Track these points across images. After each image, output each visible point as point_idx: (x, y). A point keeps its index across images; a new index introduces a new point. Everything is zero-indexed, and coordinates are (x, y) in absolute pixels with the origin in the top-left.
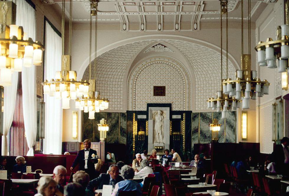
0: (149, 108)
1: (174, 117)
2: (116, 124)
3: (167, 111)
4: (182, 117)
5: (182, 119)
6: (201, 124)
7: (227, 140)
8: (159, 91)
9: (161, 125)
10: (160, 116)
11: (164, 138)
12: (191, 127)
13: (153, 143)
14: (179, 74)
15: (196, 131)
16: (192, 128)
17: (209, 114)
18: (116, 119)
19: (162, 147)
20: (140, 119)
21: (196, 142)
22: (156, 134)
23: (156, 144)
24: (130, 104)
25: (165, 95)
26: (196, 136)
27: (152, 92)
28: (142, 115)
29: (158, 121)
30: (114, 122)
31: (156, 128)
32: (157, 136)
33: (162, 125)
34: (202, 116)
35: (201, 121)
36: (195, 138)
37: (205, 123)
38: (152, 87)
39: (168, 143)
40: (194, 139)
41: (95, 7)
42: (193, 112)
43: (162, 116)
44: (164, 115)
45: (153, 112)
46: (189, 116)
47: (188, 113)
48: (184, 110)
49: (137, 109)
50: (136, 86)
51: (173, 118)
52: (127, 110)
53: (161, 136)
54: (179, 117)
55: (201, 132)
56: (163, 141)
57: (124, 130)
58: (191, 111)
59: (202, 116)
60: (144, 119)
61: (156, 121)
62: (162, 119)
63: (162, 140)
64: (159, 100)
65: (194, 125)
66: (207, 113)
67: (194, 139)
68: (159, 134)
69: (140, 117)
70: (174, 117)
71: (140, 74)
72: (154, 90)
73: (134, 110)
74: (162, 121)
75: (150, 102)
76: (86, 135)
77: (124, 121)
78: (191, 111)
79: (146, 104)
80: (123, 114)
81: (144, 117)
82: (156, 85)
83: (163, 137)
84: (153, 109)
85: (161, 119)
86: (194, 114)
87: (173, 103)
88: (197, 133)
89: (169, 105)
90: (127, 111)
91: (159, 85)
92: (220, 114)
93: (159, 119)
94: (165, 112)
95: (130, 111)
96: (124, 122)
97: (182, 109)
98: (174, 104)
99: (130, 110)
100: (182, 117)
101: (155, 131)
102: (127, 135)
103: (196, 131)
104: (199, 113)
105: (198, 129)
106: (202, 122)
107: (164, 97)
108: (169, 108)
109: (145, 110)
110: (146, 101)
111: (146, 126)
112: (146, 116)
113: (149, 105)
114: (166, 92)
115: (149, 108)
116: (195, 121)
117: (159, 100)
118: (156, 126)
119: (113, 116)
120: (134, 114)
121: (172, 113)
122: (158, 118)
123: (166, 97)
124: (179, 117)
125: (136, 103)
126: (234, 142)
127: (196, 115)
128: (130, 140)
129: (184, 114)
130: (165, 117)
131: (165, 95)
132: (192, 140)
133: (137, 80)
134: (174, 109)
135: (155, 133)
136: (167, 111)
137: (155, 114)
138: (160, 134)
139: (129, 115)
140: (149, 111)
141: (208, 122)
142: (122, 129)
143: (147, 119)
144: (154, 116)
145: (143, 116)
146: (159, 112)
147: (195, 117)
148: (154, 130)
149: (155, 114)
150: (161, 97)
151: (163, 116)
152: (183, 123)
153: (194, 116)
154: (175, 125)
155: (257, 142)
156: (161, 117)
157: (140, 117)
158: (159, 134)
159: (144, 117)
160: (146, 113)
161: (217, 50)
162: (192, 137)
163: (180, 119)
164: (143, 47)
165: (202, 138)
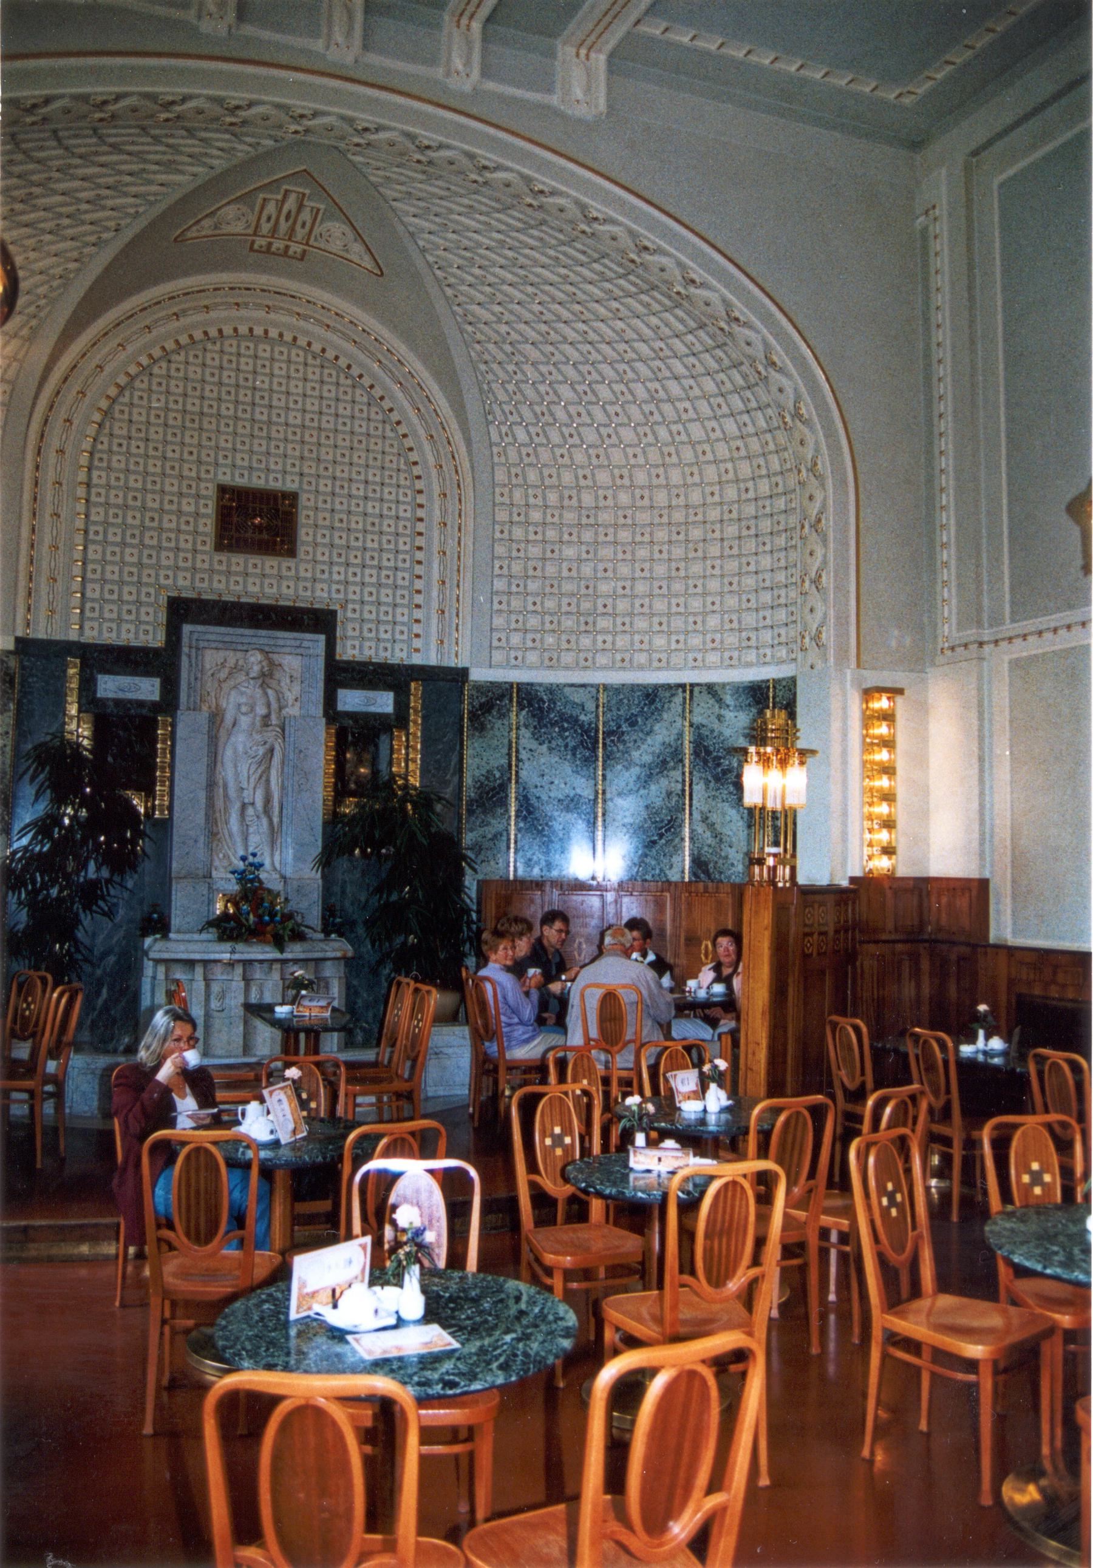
1: (351, 700)
4: (402, 706)
5: (400, 719)
6: (524, 755)
8: (257, 520)
10: (259, 692)
14: (388, 427)
16: (468, 780)
17: (577, 697)
20: (117, 702)
25: (292, 553)
27: (208, 526)
28: (134, 673)
31: (227, 772)
33: (272, 751)
34: (530, 704)
35: (526, 739)
36: (486, 845)
37: (550, 749)
38: (209, 491)
45: (211, 658)
48: (417, 660)
49: (91, 636)
50: (95, 474)
51: (340, 707)
54: (384, 702)
56: (277, 858)
58: (464, 672)
59: (530, 704)
60: (141, 704)
66: (567, 690)
67: (478, 848)
69: (109, 686)
70: (351, 700)
71: (127, 393)
72: (224, 517)
73: (73, 636)
75: (185, 586)
78: (464, 672)
79: (163, 601)
81: (148, 689)
82: (240, 482)
85: (261, 710)
86: (479, 687)
87: (344, 607)
88: (500, 811)
90: (18, 640)
91: (258, 482)
92: (653, 702)
93: (252, 709)
104: (511, 684)
105: (503, 787)
106: (534, 745)
108: (322, 638)
109: (156, 639)
111: (155, 750)
112: (157, 682)
121: (340, 674)
124: (384, 702)
127: (495, 699)
133: (106, 431)
134: (349, 651)
135: (219, 804)
136: (300, 659)
137: (223, 675)
141: (572, 744)
143: (169, 703)
144: (210, 685)
145: (137, 679)
147: (487, 707)
149: (223, 675)
150: (270, 564)
153: (482, 705)
156: (266, 694)
157: (109, 686)
160: (160, 662)
163: (387, 715)
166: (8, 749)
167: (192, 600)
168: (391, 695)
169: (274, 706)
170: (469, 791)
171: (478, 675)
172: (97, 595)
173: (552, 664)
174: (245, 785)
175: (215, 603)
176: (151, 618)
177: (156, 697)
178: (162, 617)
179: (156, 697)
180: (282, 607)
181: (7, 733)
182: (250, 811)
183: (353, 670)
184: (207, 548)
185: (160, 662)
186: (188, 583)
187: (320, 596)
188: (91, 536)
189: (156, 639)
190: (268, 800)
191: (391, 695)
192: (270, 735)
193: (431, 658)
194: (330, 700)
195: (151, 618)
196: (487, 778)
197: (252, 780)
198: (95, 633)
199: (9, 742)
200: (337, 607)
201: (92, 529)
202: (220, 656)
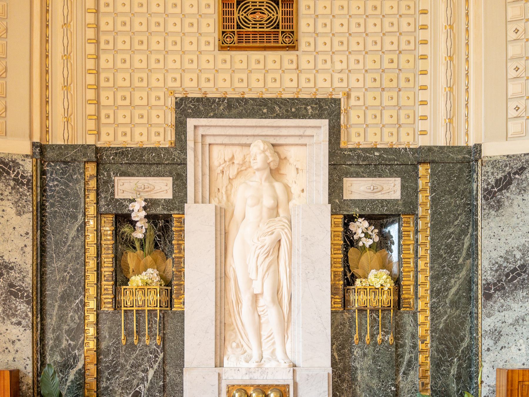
0: (191, 122)
3: (308, 147)
9: (268, 240)
10: (266, 185)
11: (296, 329)
12: (473, 252)
13: (219, 364)
22: (238, 301)
24: (57, 109)
25: (293, 47)
26: (510, 316)
29: (252, 214)
31: (236, 263)
32: (244, 316)
36: (506, 330)
40: (497, 335)
43: (278, 186)
44: (289, 173)
45: (219, 155)
47: (456, 166)
48: (423, 142)
49: (108, 139)
52: (36, 139)
53: (271, 316)
54: (390, 189)
56: (288, 346)
57: (12, 273)
61: (238, 214)
62: (276, 199)
63: (277, 339)
67: (497, 335)
68: (255, 298)
73: (91, 140)
74: (278, 215)
77: (11, 211)
79: (171, 102)
81: (162, 188)
84: (215, 142)
85: (268, 202)
87: (348, 96)
89: (328, 109)
93: (259, 201)
94: (293, 153)
95: (53, 147)
96: (16, 220)
97: (407, 139)
98: (353, 102)
99: (57, 138)
100: (410, 191)
101: (232, 283)
102: (41, 312)
107: (288, 56)
109: (164, 139)
110: (170, 84)
112: (169, 180)
115: (191, 122)
116: (507, 211)
120: (91, 169)
121: (343, 163)
122: (249, 197)
123: (304, 56)
124: (390, 189)
125: (103, 94)
128: (64, 344)
129: (422, 170)
130: (295, 190)
131: (293, 47)
132: (486, 342)
134: (354, 138)
135: (232, 295)
137: (232, 171)
138: (265, 301)
140: (190, 144)
143: (180, 198)
144: (221, 182)
145: (151, 180)
146: (258, 152)
148: (222, 277)
151: (287, 188)
158: (255, 298)
159: (162, 188)
162: (486, 323)
166: (29, 249)
167: (198, 100)
168: (399, 180)
169: (282, 197)
171: (490, 151)
172: (111, 102)
174: (253, 276)
175: (222, 100)
176: (161, 121)
177: (169, 196)
178: (171, 118)
179: (169, 196)
180: (285, 99)
181: (27, 234)
182: (262, 302)
183: (359, 156)
184: (211, 47)
185: (169, 162)
186: (194, 84)
187: (322, 87)
188: (103, 46)
190: (277, 291)
191: (399, 180)
192: (278, 226)
193: (439, 139)
194: (335, 189)
195: (161, 121)
196: (506, 260)
197: (260, 270)
198: (111, 138)
199: (29, 243)
200: (340, 95)
201: (103, 39)
202: (228, 152)
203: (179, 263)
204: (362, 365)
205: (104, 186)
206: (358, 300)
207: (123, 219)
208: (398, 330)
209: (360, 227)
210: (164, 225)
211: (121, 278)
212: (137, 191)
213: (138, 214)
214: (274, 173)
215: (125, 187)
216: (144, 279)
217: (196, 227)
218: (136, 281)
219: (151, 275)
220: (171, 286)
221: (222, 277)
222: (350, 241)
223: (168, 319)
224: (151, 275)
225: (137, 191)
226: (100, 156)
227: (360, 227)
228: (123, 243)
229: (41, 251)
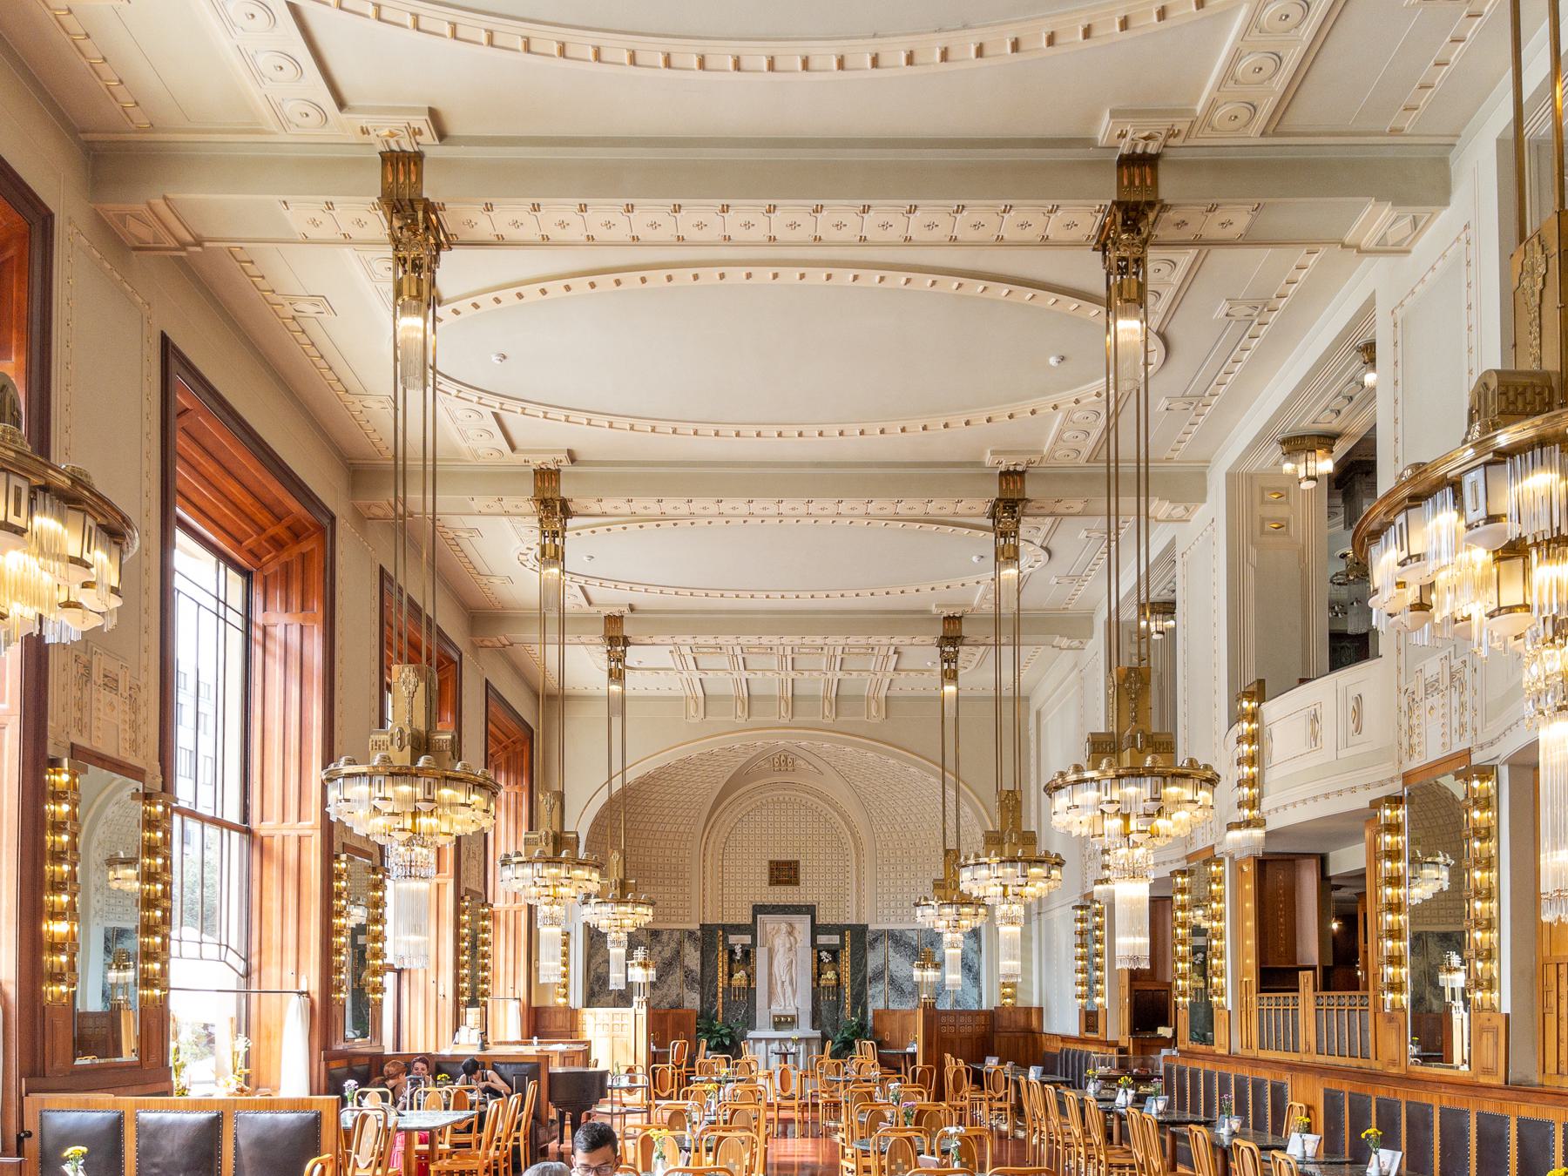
1: (823, 939)
2: (673, 958)
3: (803, 924)
4: (842, 940)
7: (957, 1002)
8: (784, 873)
11: (798, 995)
15: (878, 976)
17: (910, 934)
18: (673, 945)
19: (793, 1017)
21: (880, 1005)
23: (777, 1009)
24: (708, 911)
25: (797, 884)
27: (766, 877)
30: (667, 953)
38: (766, 863)
39: (807, 1007)
41: (619, 660)
42: (871, 927)
46: (859, 936)
47: (859, 931)
53: (789, 990)
54: (835, 940)
55: (892, 981)
64: (784, 895)
65: (873, 960)
70: (823, 939)
75: (759, 900)
76: (597, 988)
80: (691, 933)
81: (747, 939)
83: (794, 992)
84: (768, 923)
89: (810, 910)
97: (841, 921)
100: (842, 940)
103: (878, 976)
109: (749, 921)
113: (759, 909)
114: (802, 877)
117: (784, 895)
118: (776, 963)
119: (665, 937)
121: (816, 930)
122: (780, 942)
123: (802, 888)
126: (976, 1007)
127: (879, 936)
131: (797, 884)
134: (820, 921)
139: (709, 937)
142: (688, 973)
143: (754, 944)
146: (784, 927)
147: (876, 940)
148: (770, 974)
150: (789, 888)
152: (846, 956)
154: (826, 956)
155: (1035, 1003)
159: (747, 939)
161: (933, 773)
162: (870, 992)
164: (743, 760)
165: (893, 995)
170: (870, 974)
173: (902, 921)
185: (751, 929)
187: (808, 900)
189: (749, 921)
192: (791, 954)
194: (813, 940)
203: (754, 970)
204: (824, 1008)
205: (725, 939)
206: (822, 983)
207: (732, 952)
208: (838, 995)
209: (824, 954)
210: (748, 954)
211: (731, 976)
212: (739, 941)
213: (738, 949)
214: (790, 933)
215: (733, 939)
216: (740, 976)
217: (761, 955)
218: (737, 976)
219: (742, 973)
220: (750, 977)
221: (770, 974)
222: (820, 960)
223: (750, 992)
224: (742, 973)
225: (739, 941)
226: (724, 927)
227: (824, 954)
228: (731, 960)
229: (702, 964)
